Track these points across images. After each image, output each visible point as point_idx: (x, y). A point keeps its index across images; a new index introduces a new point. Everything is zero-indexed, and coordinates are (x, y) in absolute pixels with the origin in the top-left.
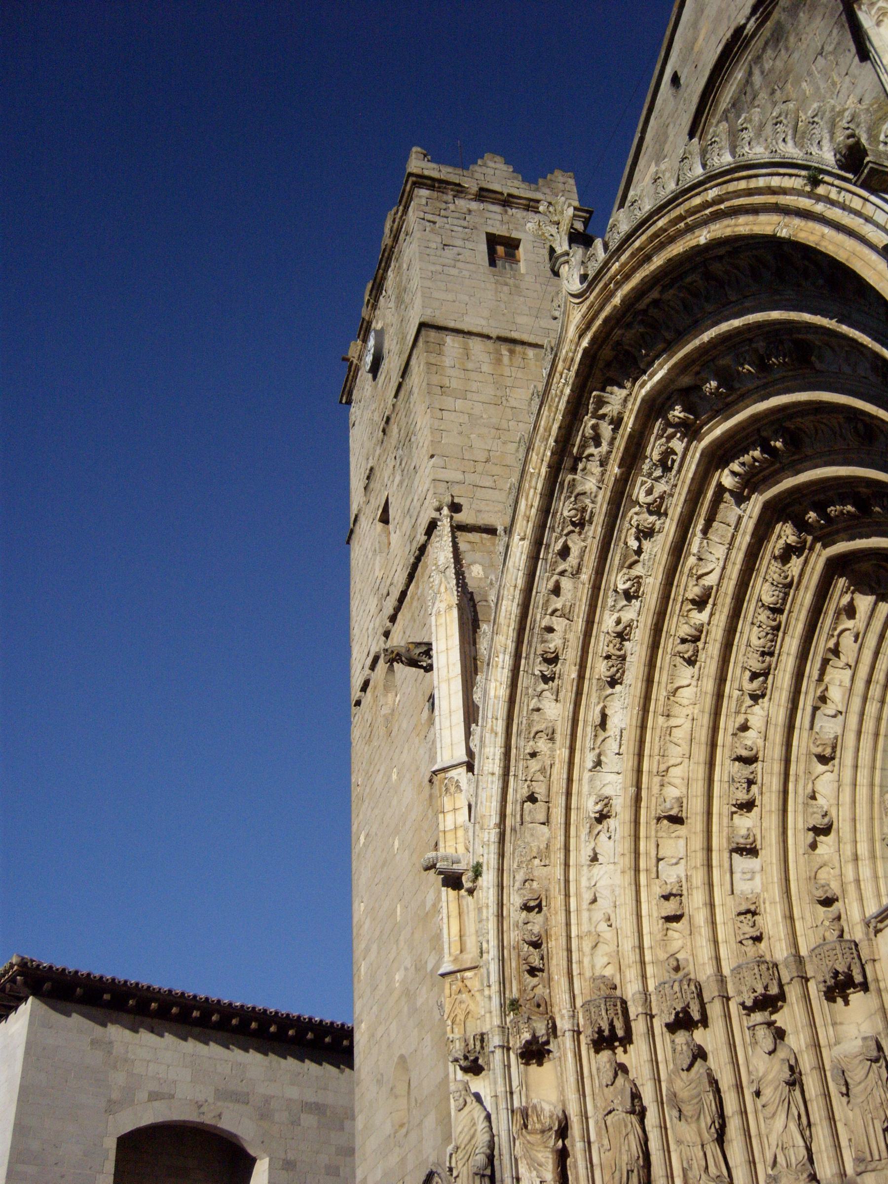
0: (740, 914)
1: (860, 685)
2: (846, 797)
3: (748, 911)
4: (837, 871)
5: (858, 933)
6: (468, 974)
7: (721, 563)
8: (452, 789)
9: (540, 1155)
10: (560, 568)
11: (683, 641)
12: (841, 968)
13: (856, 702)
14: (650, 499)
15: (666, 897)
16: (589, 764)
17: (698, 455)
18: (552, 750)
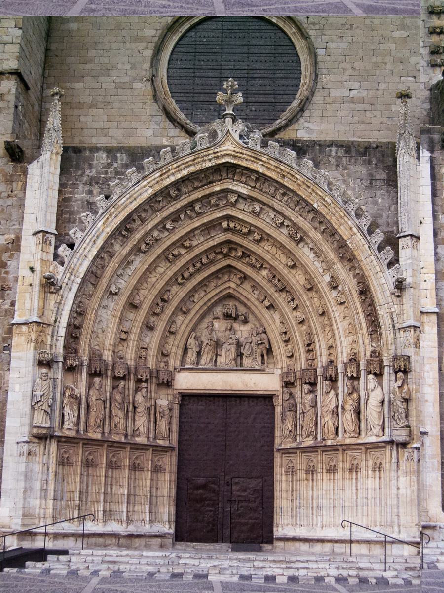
0: (143, 348)
1: (206, 299)
2: (183, 327)
3: (146, 349)
4: (170, 347)
5: (171, 369)
6: (45, 326)
7: (200, 242)
8: (48, 242)
9: (75, 407)
10: (153, 204)
11: (173, 256)
12: (169, 380)
13: (201, 303)
14: (200, 211)
15: (126, 332)
16: (119, 273)
17: (225, 213)
18: (109, 261)
